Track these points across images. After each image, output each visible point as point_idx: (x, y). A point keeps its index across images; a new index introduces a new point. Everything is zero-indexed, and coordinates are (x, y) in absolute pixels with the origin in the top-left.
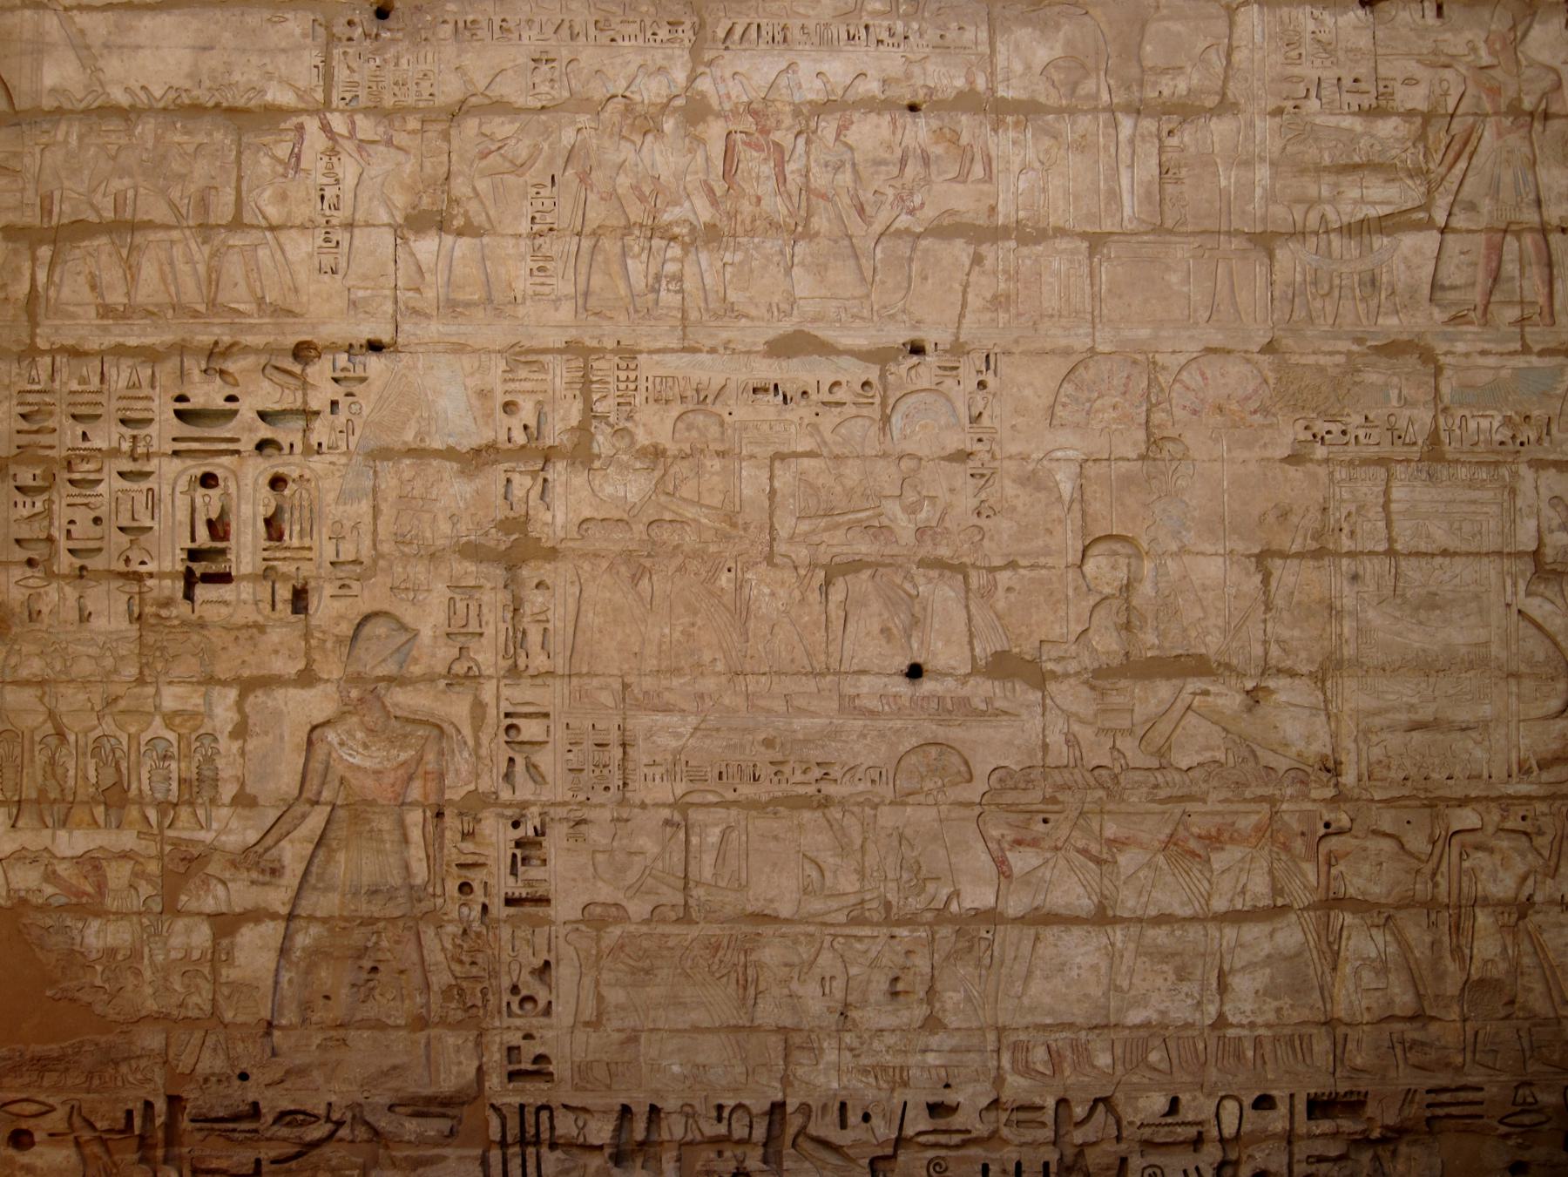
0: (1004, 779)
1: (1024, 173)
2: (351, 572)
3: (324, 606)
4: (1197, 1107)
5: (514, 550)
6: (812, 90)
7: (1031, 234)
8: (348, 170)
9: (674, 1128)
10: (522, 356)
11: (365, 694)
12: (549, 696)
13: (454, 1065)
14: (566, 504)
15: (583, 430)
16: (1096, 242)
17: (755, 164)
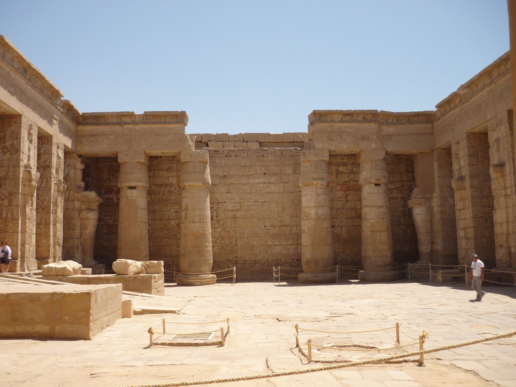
0: (272, 235)
1: (273, 188)
2: (223, 219)
3: (221, 222)
4: (287, 260)
5: (235, 218)
6: (257, 182)
7: (274, 193)
8: (222, 189)
9: (247, 262)
10: (235, 203)
11: (224, 229)
12: (238, 229)
13: (231, 257)
14: (239, 214)
15: (240, 208)
16: (279, 193)
17: (253, 188)
